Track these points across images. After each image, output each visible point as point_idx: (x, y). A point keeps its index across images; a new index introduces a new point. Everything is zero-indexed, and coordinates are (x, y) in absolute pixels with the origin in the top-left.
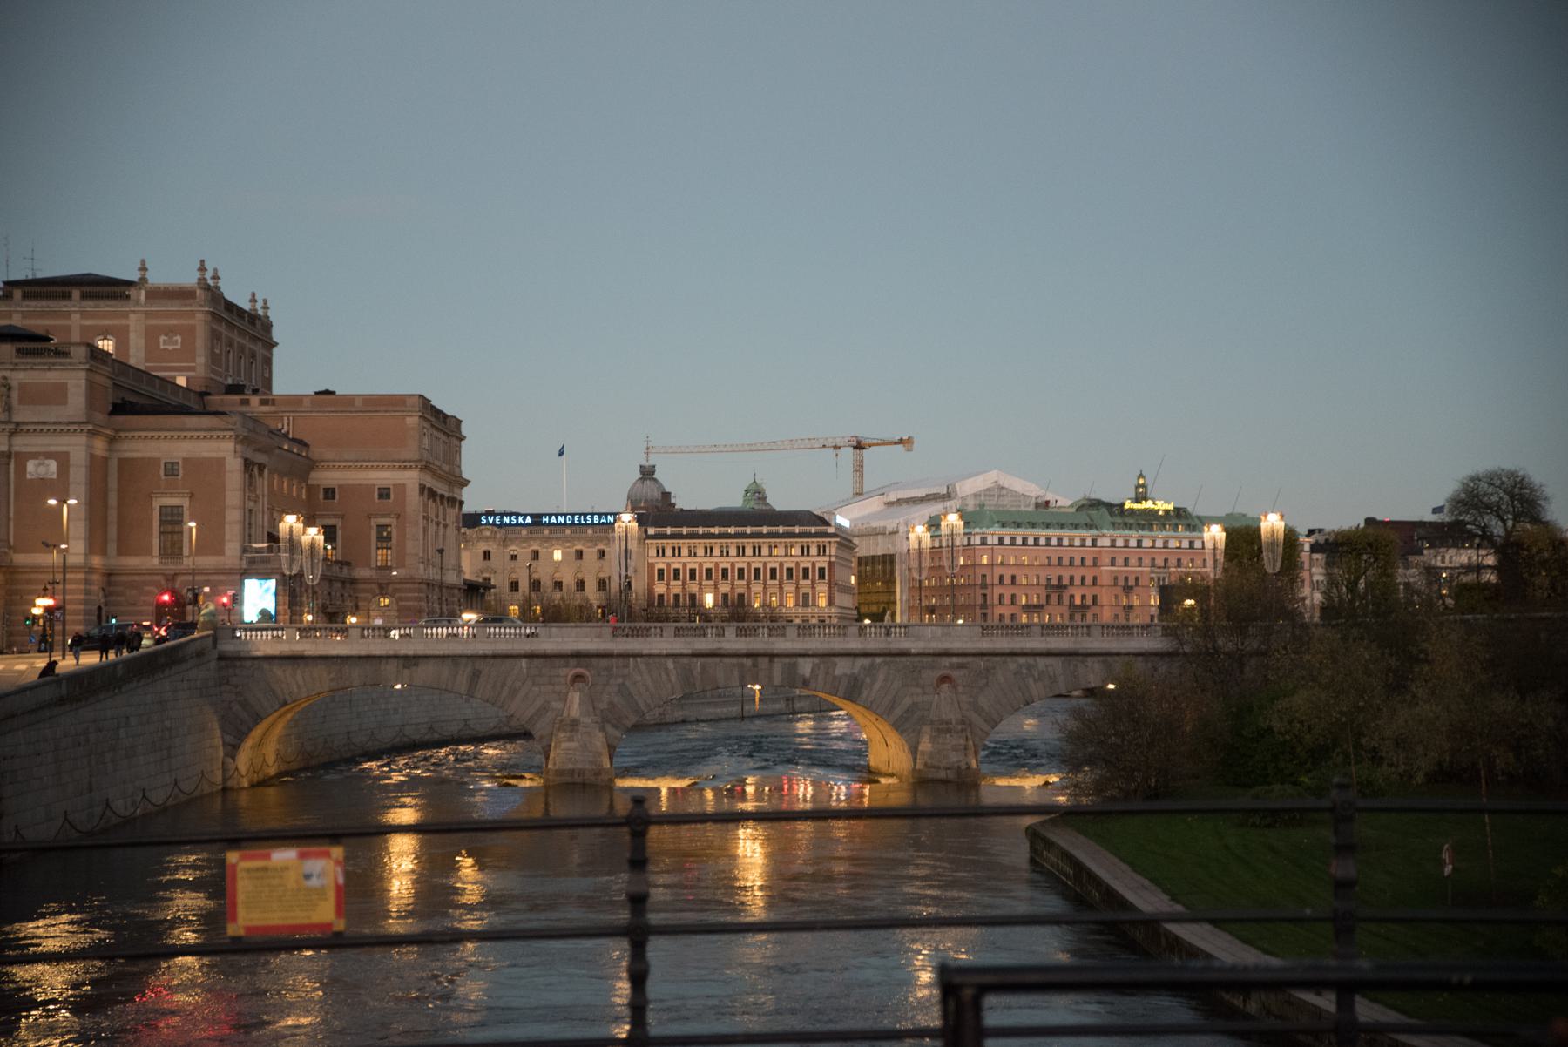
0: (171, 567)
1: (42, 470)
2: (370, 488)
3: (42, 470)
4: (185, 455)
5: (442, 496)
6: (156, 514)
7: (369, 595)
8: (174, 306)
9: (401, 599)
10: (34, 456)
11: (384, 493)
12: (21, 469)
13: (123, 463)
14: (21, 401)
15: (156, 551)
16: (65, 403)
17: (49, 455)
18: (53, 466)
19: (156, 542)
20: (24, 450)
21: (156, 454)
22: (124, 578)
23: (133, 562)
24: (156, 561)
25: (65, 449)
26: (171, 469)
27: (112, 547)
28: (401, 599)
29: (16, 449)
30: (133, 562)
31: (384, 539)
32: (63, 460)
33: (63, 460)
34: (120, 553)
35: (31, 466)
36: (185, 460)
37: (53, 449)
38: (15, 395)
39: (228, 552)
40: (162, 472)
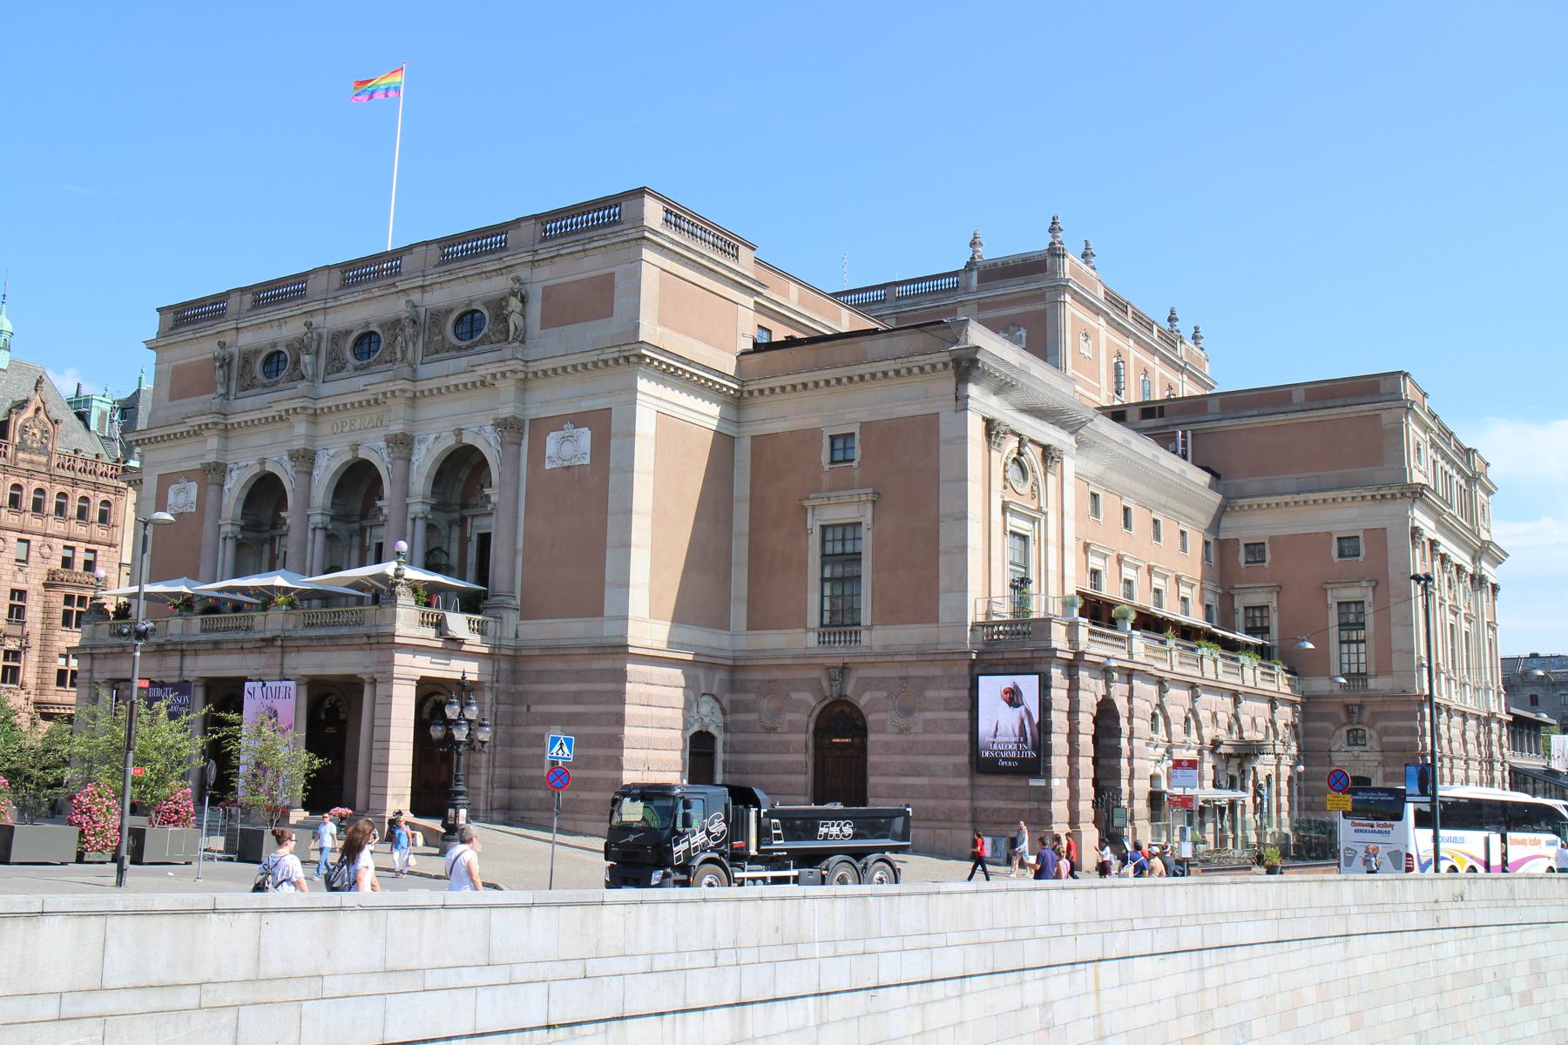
0: (840, 652)
2: (1318, 541)
3: (568, 449)
4: (866, 417)
5: (1459, 568)
6: (814, 541)
7: (1329, 726)
8: (1012, 288)
9: (1385, 732)
10: (557, 423)
11: (1348, 546)
13: (760, 443)
14: (546, 323)
15: (813, 619)
17: (579, 419)
18: (585, 437)
19: (813, 598)
22: (758, 675)
23: (774, 640)
24: (812, 639)
27: (739, 613)
28: (1385, 732)
29: (533, 413)
30: (774, 640)
31: (1351, 622)
34: (752, 625)
35: (552, 442)
36: (865, 426)
38: (535, 309)
39: (941, 619)
40: (825, 457)
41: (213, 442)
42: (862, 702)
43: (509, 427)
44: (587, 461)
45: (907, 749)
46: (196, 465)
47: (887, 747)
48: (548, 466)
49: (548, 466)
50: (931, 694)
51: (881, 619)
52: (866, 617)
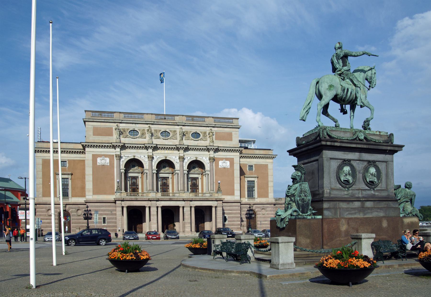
0: (251, 201)
1: (224, 164)
3: (224, 164)
4: (255, 163)
10: (222, 159)
12: (217, 165)
16: (231, 140)
17: (227, 159)
18: (228, 163)
20: (218, 157)
21: (246, 163)
25: (232, 157)
26: (251, 167)
32: (232, 161)
33: (232, 161)
35: (221, 163)
37: (228, 157)
39: (269, 197)
40: (248, 169)
41: (118, 150)
42: (256, 210)
43: (213, 160)
44: (229, 167)
45: (264, 217)
46: (114, 154)
47: (261, 217)
48: (220, 167)
49: (220, 167)
50: (268, 209)
51: (259, 196)
52: (256, 196)
